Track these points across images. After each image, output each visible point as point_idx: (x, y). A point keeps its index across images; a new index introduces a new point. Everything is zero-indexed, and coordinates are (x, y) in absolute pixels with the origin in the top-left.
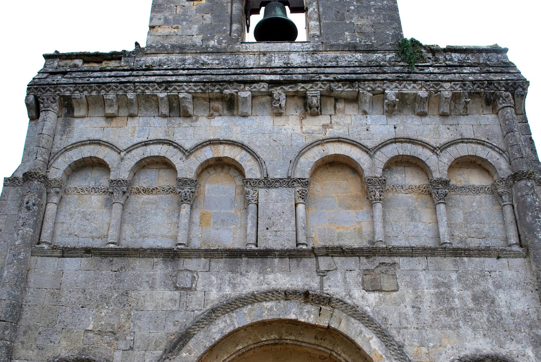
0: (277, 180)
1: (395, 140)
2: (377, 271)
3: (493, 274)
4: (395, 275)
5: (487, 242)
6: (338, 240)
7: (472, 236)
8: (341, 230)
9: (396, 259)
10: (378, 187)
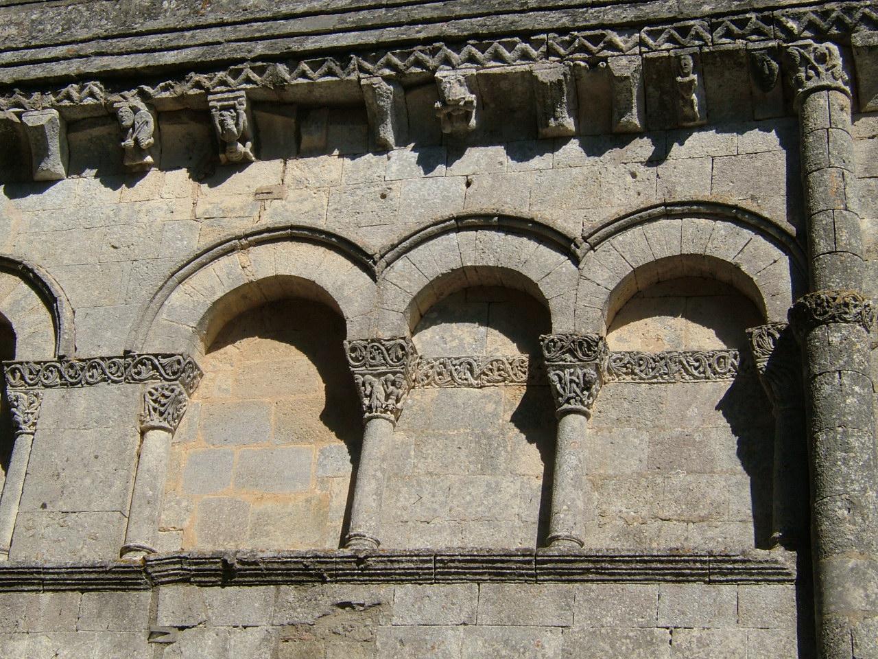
0: (92, 364)
1: (462, 223)
2: (323, 627)
3: (681, 637)
4: (373, 640)
5: (709, 534)
6: (253, 537)
7: (666, 514)
8: (268, 506)
9: (381, 591)
10: (383, 369)
